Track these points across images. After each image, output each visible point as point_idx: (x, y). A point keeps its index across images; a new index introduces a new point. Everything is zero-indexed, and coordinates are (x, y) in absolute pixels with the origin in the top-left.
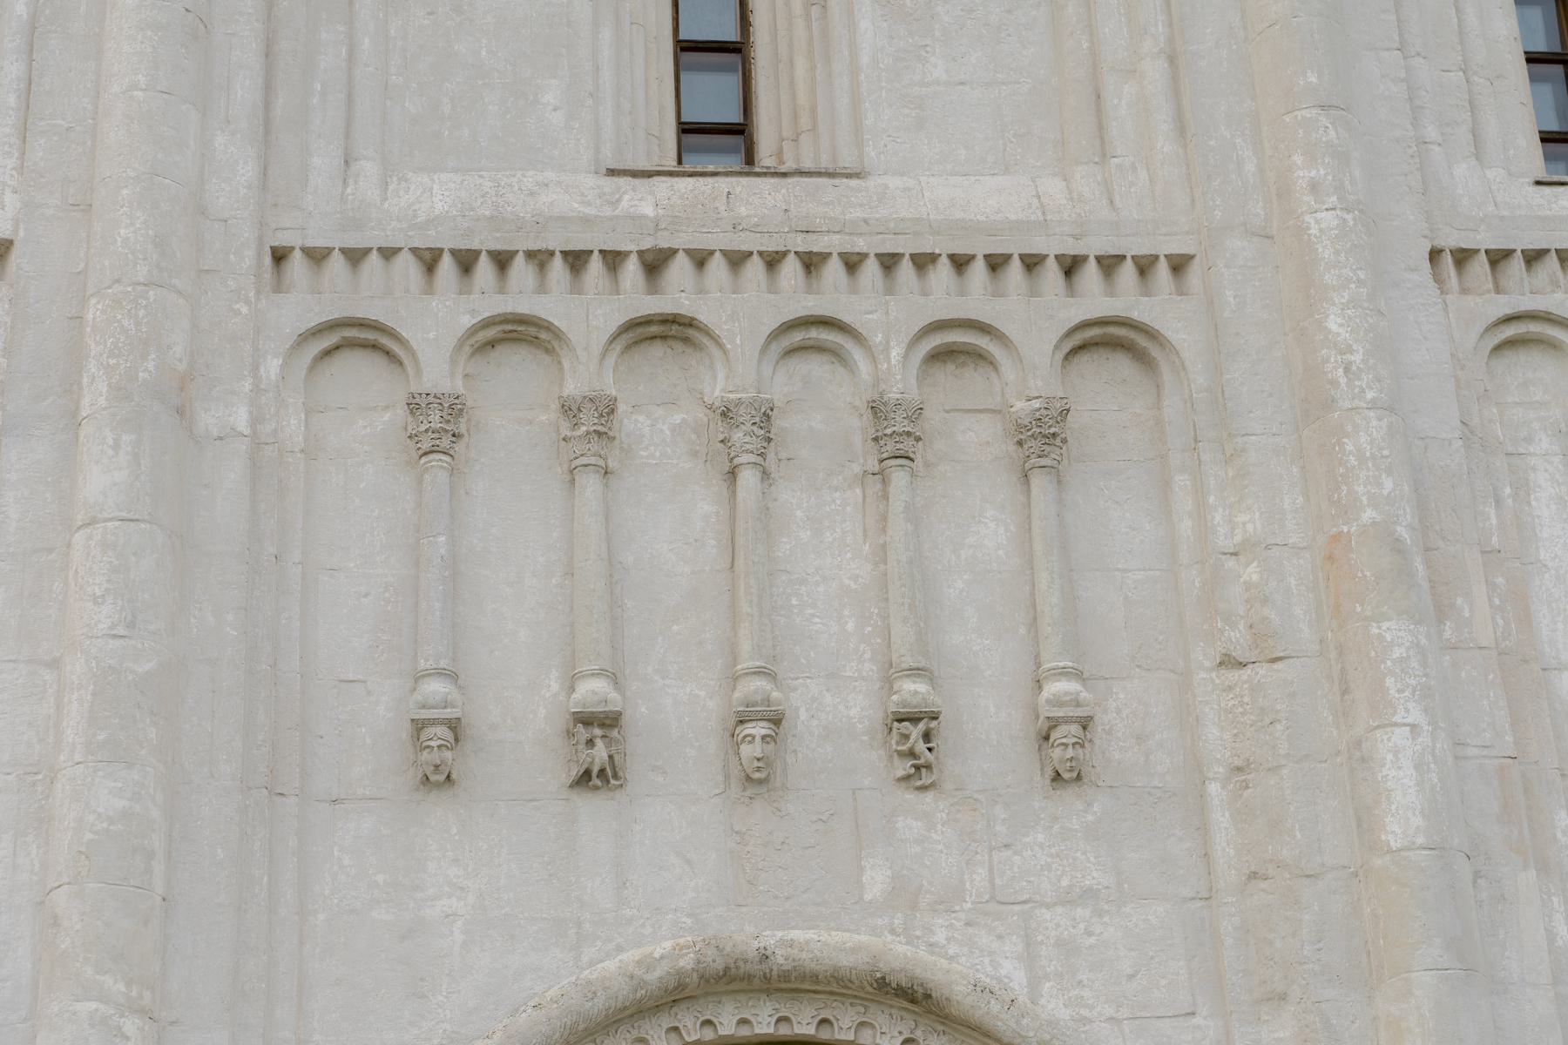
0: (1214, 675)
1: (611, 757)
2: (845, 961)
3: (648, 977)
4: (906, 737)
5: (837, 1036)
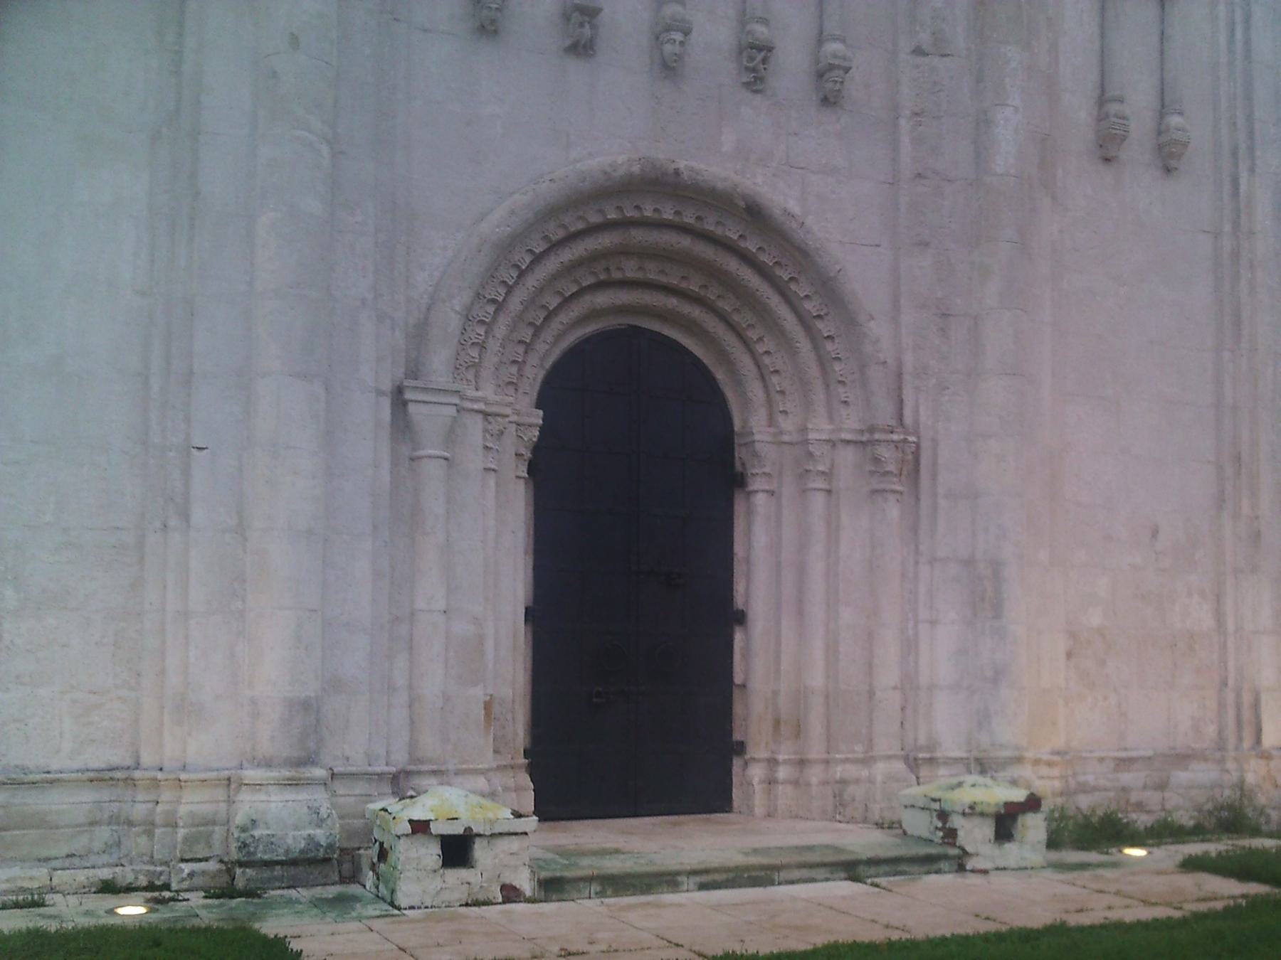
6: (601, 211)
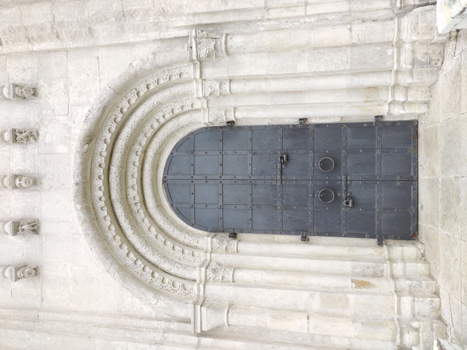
0: (4, 47)
1: (29, 224)
2: (79, 161)
3: (83, 218)
4: (22, 139)
5: (103, 162)
6: (105, 217)
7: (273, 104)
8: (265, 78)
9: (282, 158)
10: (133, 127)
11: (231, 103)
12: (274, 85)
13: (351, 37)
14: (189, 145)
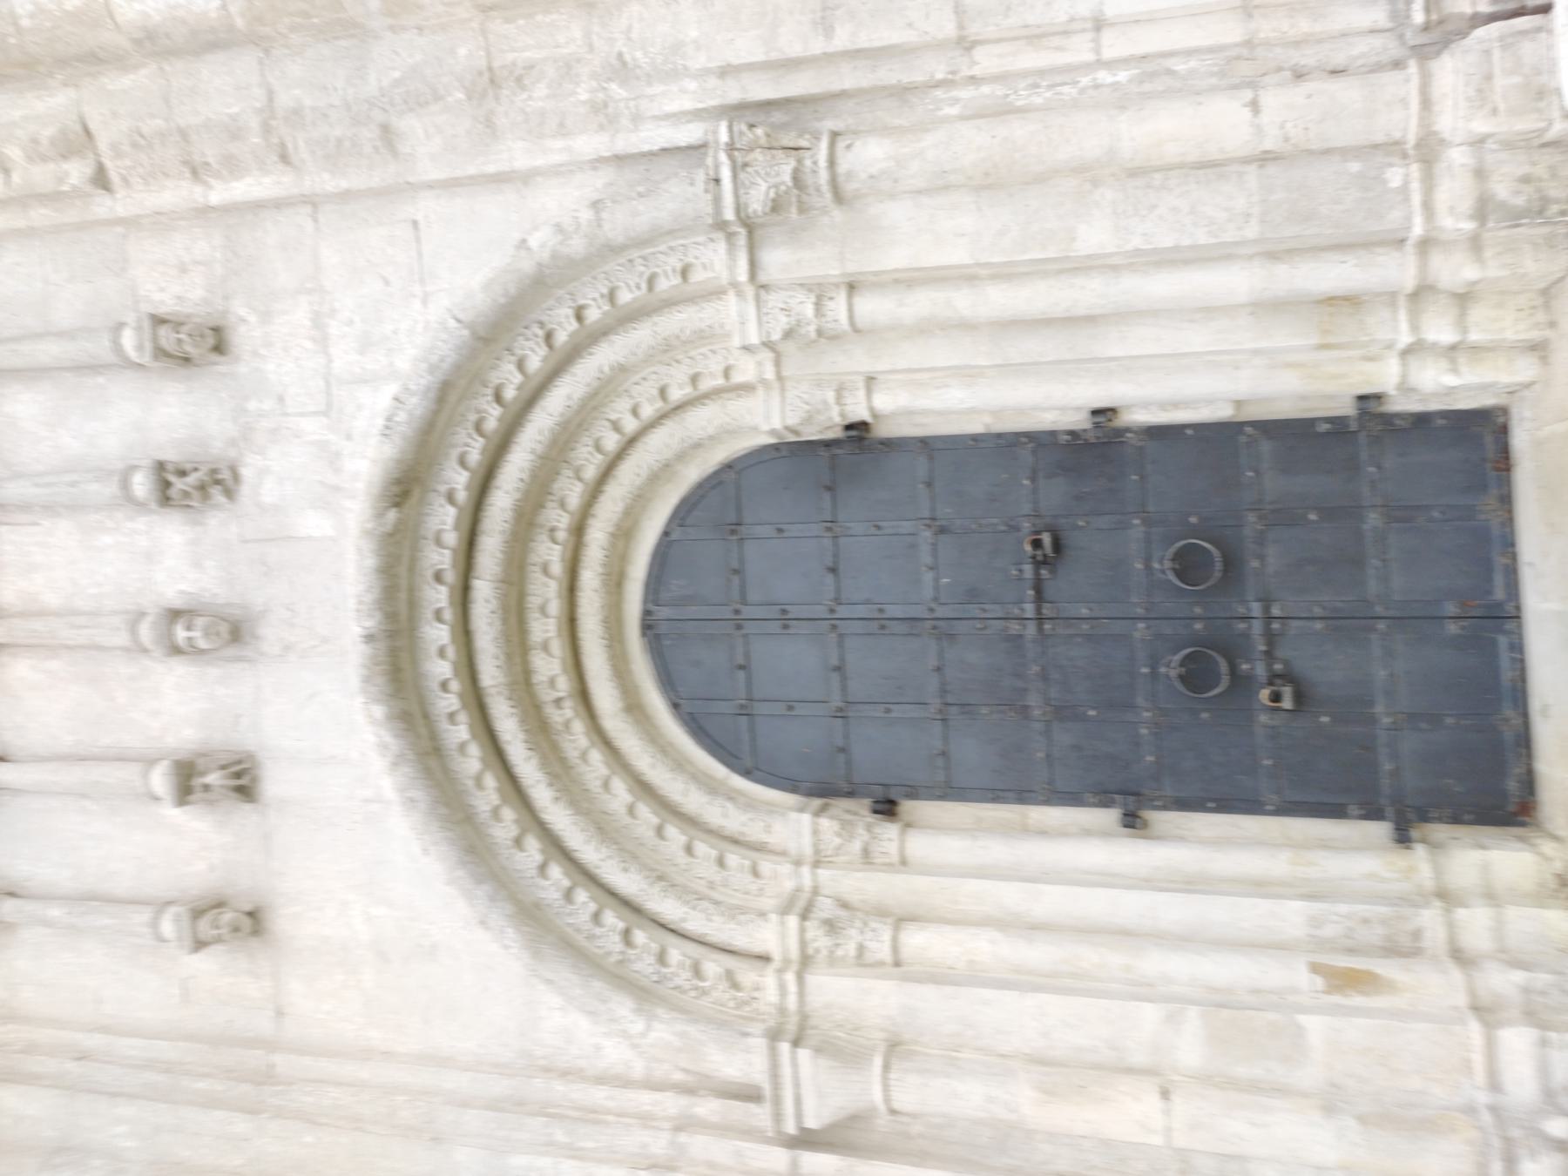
1: (223, 767)
6: (462, 747)
7: (999, 362)
8: (967, 276)
9: (1037, 544)
10: (539, 449)
11: (854, 361)
12: (1000, 300)
13: (1259, 130)
14: (726, 503)
